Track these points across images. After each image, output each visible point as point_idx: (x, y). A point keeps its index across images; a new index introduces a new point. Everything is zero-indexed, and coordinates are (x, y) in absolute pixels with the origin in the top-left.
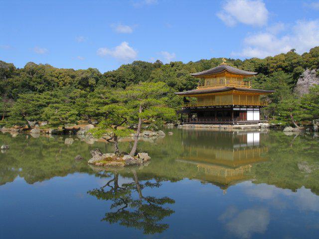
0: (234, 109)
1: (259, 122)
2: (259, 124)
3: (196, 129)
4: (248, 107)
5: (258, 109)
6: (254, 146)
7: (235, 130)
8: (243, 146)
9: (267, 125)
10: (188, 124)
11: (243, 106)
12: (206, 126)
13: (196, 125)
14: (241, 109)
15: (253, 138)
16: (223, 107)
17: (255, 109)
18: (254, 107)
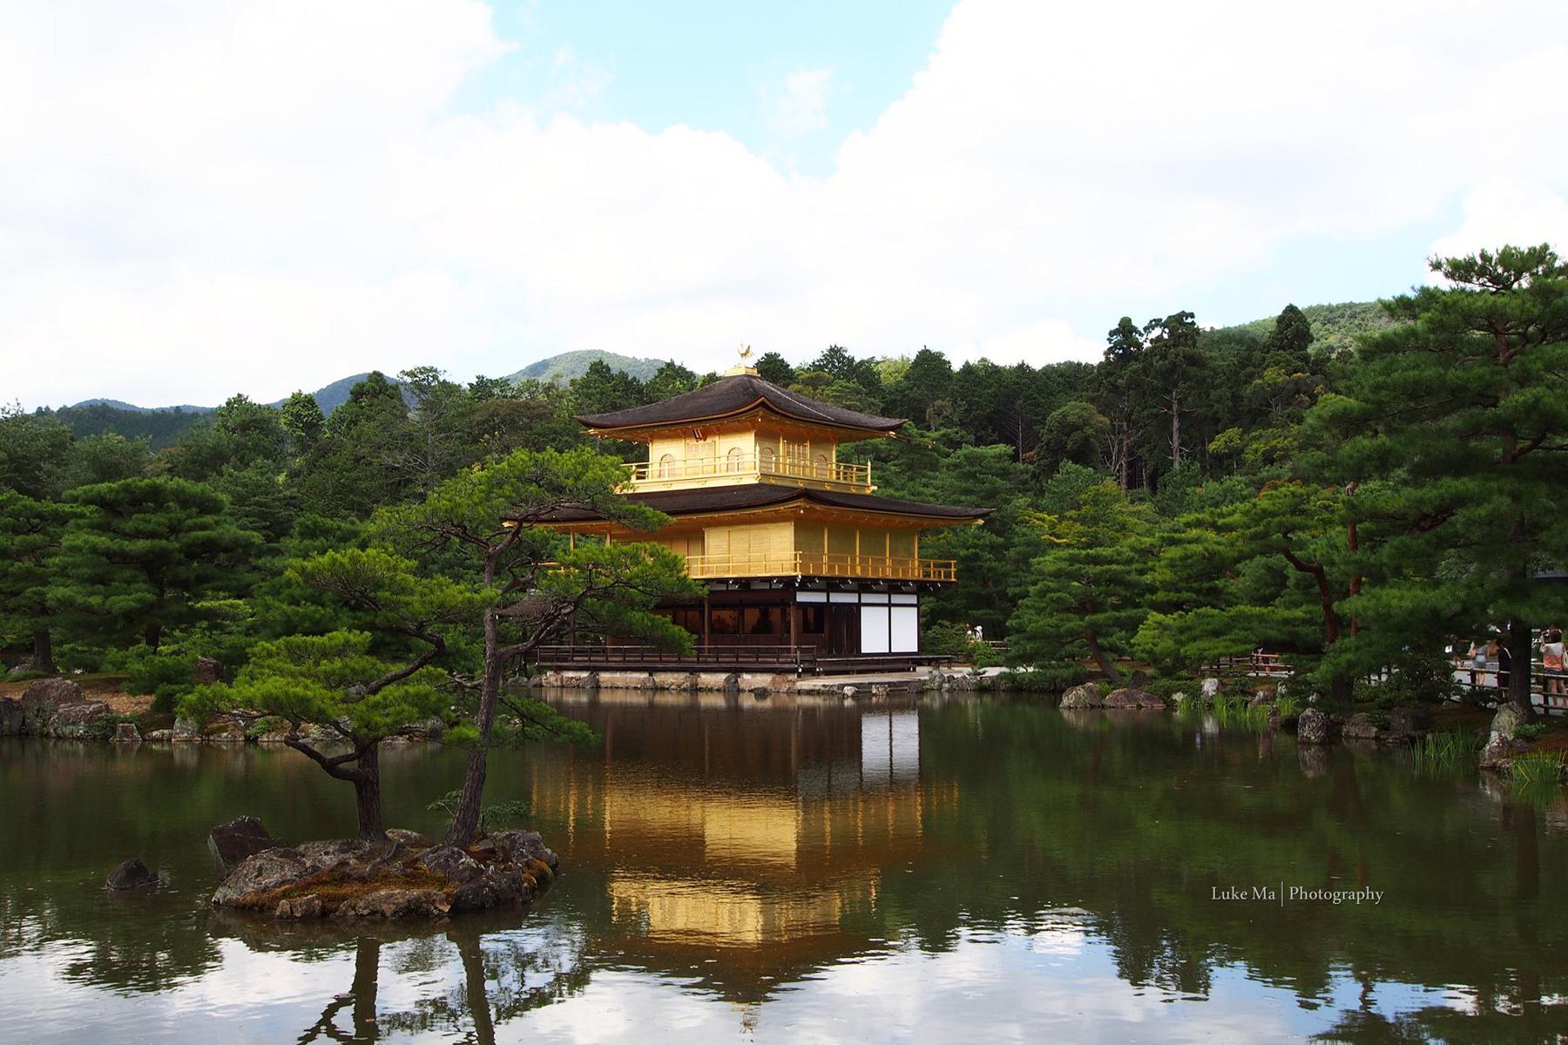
0: (802, 597)
1: (920, 663)
2: (923, 673)
3: (605, 698)
4: (864, 586)
5: (913, 599)
6: (893, 782)
7: (806, 701)
8: (843, 778)
9: (962, 672)
10: (558, 670)
11: (844, 580)
12: (660, 678)
13: (605, 677)
14: (836, 598)
15: (890, 742)
16: (745, 583)
17: (896, 599)
18: (894, 587)
